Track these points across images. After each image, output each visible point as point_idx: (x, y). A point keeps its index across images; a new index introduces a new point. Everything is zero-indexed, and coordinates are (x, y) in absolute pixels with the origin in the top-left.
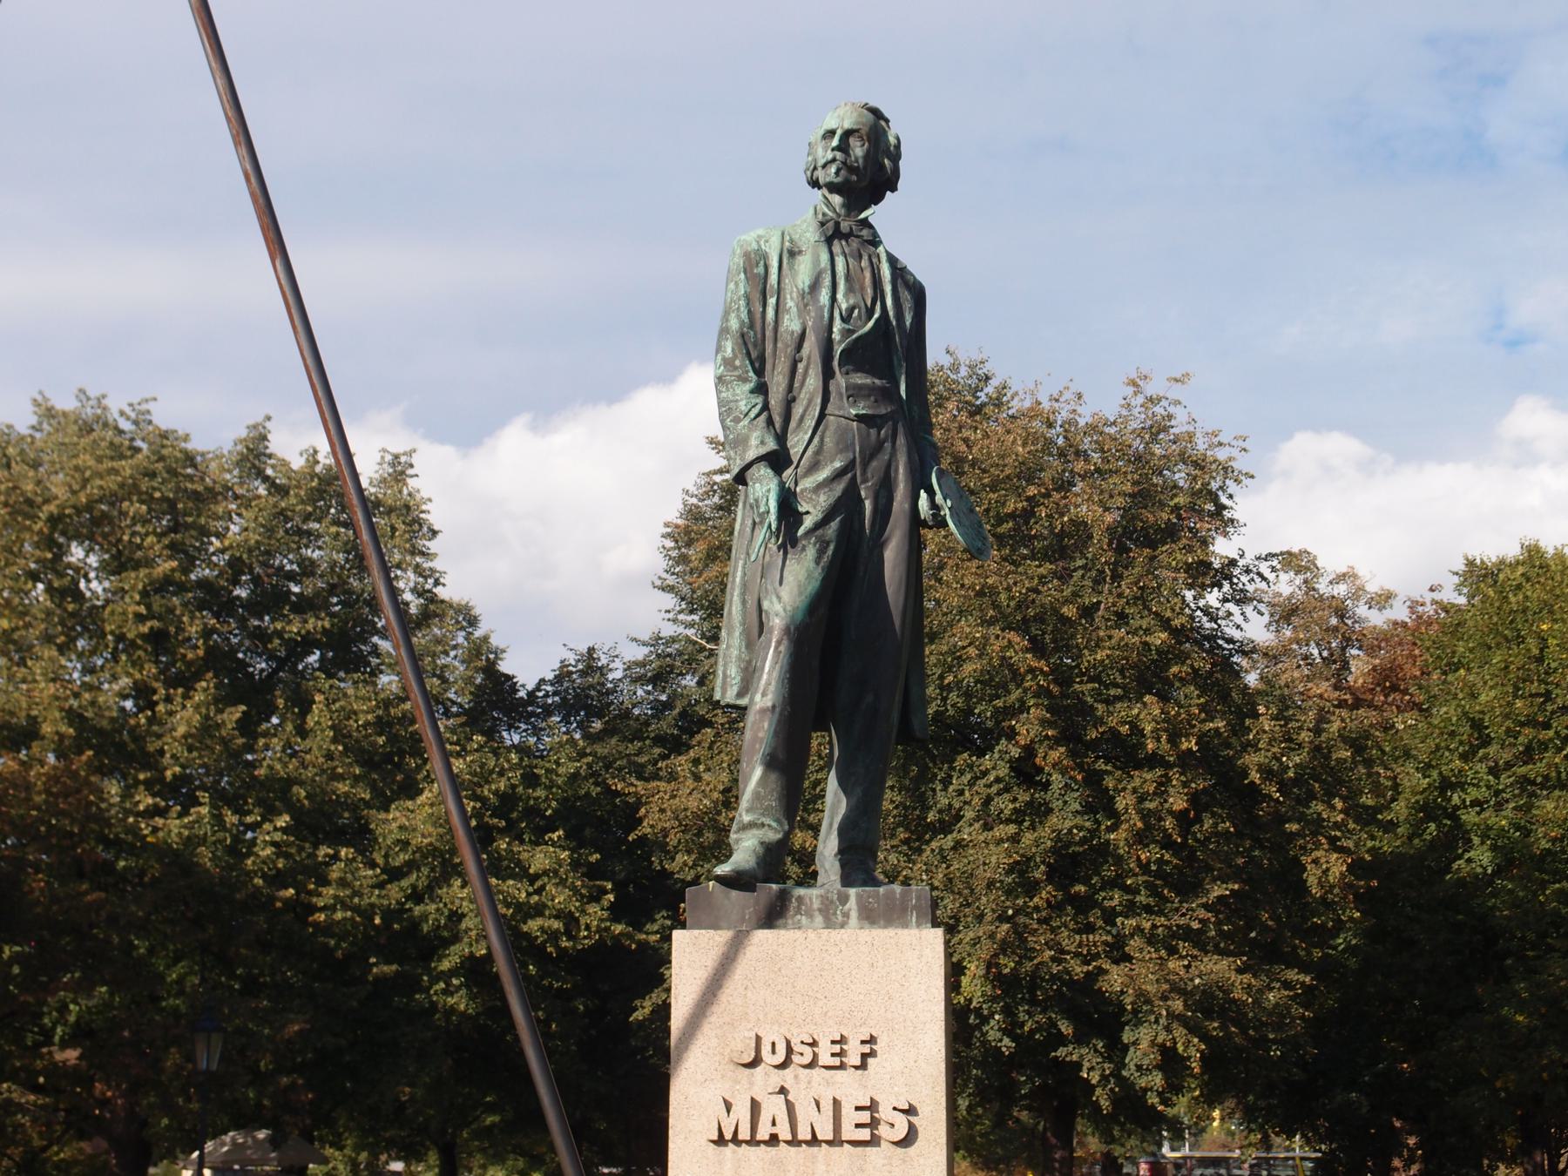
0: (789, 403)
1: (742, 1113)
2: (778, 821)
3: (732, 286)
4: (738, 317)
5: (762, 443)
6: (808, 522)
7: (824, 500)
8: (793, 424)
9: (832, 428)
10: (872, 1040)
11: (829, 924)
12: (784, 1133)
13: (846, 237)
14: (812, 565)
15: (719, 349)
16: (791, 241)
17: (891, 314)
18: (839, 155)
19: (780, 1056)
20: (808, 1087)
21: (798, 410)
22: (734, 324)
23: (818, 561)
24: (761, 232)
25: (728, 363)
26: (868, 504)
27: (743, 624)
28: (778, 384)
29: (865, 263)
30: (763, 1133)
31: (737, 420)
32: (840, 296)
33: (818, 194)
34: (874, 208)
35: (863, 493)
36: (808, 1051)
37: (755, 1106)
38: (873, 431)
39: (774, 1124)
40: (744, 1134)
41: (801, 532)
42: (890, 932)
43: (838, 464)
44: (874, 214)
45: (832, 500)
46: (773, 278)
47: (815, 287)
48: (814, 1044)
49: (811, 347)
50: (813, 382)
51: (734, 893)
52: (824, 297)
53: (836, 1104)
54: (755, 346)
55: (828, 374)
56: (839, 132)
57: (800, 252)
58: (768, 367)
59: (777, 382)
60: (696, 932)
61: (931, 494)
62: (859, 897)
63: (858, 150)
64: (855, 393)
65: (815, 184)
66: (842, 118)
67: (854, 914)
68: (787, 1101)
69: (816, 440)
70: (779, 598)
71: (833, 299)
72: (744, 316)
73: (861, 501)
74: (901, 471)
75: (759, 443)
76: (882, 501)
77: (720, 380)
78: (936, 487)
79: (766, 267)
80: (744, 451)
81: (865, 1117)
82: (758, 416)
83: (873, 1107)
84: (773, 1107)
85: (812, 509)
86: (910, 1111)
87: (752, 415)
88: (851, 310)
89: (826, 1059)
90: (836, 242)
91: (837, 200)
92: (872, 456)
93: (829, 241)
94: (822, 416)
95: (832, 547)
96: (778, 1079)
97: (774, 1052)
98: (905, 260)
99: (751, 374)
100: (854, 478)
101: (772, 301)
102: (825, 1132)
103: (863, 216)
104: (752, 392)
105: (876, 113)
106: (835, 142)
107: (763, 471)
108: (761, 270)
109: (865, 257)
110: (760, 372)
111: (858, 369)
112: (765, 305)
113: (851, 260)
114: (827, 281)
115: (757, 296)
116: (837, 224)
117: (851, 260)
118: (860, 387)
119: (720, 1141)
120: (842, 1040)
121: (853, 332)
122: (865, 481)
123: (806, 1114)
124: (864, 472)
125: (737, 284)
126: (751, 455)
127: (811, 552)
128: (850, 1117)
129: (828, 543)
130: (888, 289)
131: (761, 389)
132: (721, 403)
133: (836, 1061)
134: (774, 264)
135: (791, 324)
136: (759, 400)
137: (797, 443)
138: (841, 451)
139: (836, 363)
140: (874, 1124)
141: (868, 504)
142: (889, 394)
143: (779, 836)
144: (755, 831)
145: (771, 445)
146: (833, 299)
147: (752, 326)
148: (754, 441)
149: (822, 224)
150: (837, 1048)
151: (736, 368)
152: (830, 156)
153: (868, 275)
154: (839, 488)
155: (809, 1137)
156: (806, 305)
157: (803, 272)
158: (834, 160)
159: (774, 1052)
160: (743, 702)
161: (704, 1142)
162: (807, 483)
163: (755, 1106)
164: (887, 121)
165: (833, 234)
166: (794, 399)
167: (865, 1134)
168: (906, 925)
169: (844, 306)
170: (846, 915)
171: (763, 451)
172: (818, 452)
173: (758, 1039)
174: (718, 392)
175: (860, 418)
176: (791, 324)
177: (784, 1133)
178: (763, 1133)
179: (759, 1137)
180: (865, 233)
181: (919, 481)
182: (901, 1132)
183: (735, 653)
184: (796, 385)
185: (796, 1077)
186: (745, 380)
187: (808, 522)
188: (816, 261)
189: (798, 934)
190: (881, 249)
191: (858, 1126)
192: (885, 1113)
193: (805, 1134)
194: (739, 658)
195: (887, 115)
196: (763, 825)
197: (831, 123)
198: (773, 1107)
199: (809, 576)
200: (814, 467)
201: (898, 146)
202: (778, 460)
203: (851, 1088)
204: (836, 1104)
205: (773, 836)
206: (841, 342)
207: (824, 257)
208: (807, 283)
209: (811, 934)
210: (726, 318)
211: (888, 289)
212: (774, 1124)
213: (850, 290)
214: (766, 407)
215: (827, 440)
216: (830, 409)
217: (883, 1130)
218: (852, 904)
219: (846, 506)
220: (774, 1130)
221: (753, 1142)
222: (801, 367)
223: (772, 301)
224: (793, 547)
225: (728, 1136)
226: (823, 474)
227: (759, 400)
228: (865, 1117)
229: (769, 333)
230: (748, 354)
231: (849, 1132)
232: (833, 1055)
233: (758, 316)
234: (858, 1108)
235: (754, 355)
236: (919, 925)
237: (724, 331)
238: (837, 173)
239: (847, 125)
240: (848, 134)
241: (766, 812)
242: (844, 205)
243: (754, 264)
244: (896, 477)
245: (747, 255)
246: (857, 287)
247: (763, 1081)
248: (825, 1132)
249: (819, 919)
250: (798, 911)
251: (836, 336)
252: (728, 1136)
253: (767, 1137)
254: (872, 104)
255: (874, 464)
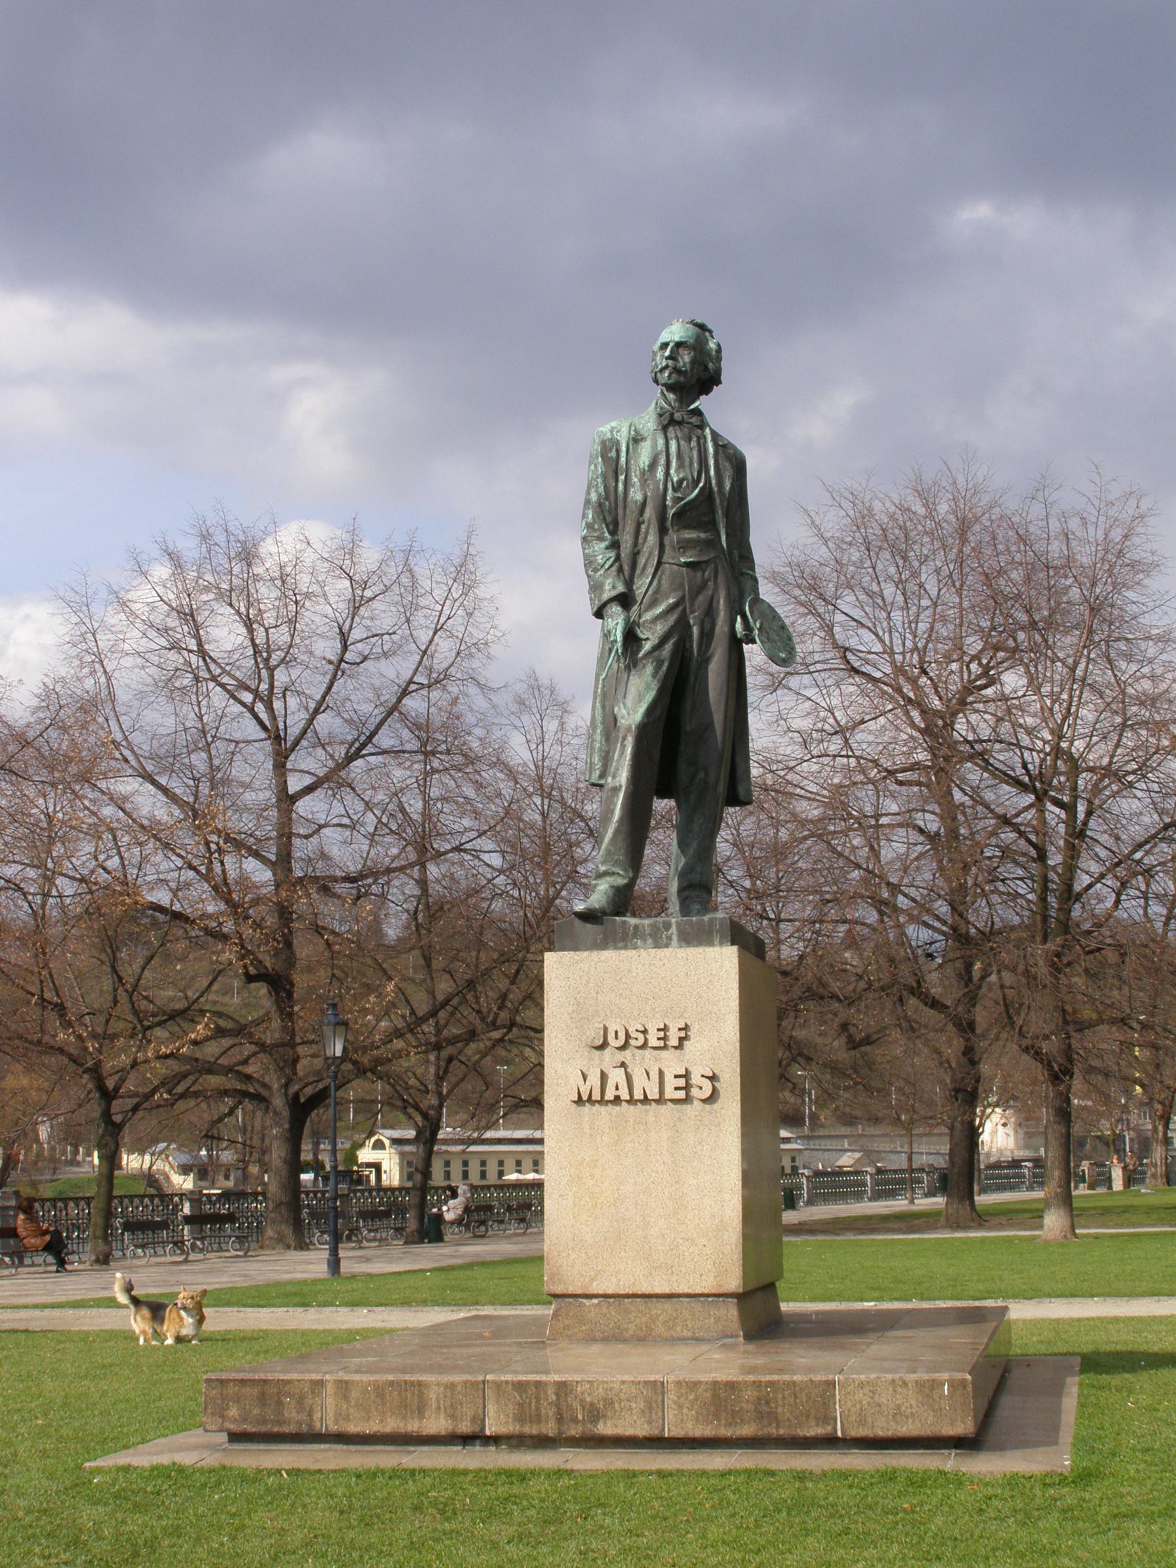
0: (635, 555)
1: (594, 1080)
2: (625, 870)
3: (592, 467)
4: (597, 491)
5: (614, 587)
6: (647, 646)
7: (660, 628)
8: (638, 571)
9: (667, 573)
10: (686, 1028)
11: (657, 945)
12: (625, 1095)
13: (680, 423)
14: (650, 678)
15: (584, 516)
16: (635, 431)
17: (714, 482)
18: (670, 362)
19: (621, 1042)
20: (640, 1063)
21: (642, 561)
22: (594, 497)
23: (654, 676)
24: (613, 424)
25: (589, 526)
26: (695, 631)
27: (603, 723)
28: (626, 542)
29: (693, 444)
30: (610, 1095)
31: (596, 570)
32: (672, 471)
33: (659, 389)
34: (703, 398)
35: (691, 621)
36: (641, 1036)
37: (604, 1077)
38: (699, 574)
39: (617, 1088)
40: (596, 1096)
41: (641, 655)
42: (700, 950)
43: (671, 601)
44: (702, 403)
45: (666, 628)
46: (623, 459)
47: (653, 465)
48: (645, 1032)
49: (649, 513)
50: (652, 539)
51: (589, 926)
52: (660, 473)
53: (661, 1073)
54: (610, 512)
55: (663, 531)
56: (671, 345)
57: (643, 439)
58: (620, 527)
59: (626, 539)
60: (561, 953)
61: (744, 617)
62: (678, 924)
63: (686, 358)
64: (684, 546)
65: (656, 381)
66: (675, 332)
67: (675, 937)
68: (627, 1074)
69: (655, 583)
70: (624, 704)
71: (667, 474)
72: (601, 490)
73: (689, 627)
74: (722, 602)
75: (612, 587)
76: (708, 626)
77: (584, 539)
78: (748, 613)
79: (618, 452)
80: (601, 594)
81: (682, 1082)
82: (611, 566)
83: (687, 1075)
84: (617, 1076)
85: (650, 637)
86: (713, 1078)
87: (607, 566)
88: (681, 481)
89: (653, 1042)
90: (671, 429)
91: (671, 396)
92: (699, 592)
93: (665, 429)
94: (659, 563)
95: (666, 664)
96: (620, 1056)
97: (616, 1038)
98: (729, 436)
99: (607, 534)
100: (684, 610)
101: (622, 478)
102: (653, 1094)
103: (692, 407)
104: (607, 548)
105: (702, 327)
106: (667, 353)
107: (616, 609)
108: (613, 454)
109: (695, 439)
110: (613, 533)
111: (688, 527)
112: (617, 481)
113: (682, 442)
114: (662, 461)
115: (611, 474)
116: (672, 415)
117: (682, 442)
118: (689, 541)
119: (579, 1101)
120: (665, 1029)
121: (683, 499)
122: (692, 612)
123: (640, 1082)
124: (692, 605)
125: (596, 466)
126: (606, 596)
127: (649, 669)
128: (671, 1083)
129: (663, 662)
130: (711, 462)
131: (615, 545)
132: (586, 556)
133: (661, 1043)
134: (624, 449)
135: (636, 495)
136: (612, 554)
137: (641, 585)
138: (675, 590)
139: (669, 523)
140: (687, 1087)
141: (695, 631)
142: (713, 543)
143: (626, 881)
144: (608, 879)
145: (621, 588)
146: (667, 474)
147: (607, 498)
148: (607, 587)
149: (661, 416)
150: (662, 1034)
151: (595, 530)
152: (664, 364)
153: (695, 453)
154: (672, 619)
155: (642, 1097)
156: (646, 481)
157: (644, 457)
158: (667, 367)
159: (616, 1038)
160: (602, 782)
161: (569, 1103)
162: (648, 616)
163: (604, 1077)
164: (710, 332)
165: (668, 422)
166: (638, 553)
167: (681, 1094)
168: (711, 944)
169: (675, 479)
170: (669, 938)
171: (614, 593)
172: (657, 592)
173: (605, 1029)
174: (584, 549)
175: (688, 565)
176: (636, 495)
177: (625, 1095)
178: (610, 1095)
179: (606, 1098)
180: (694, 420)
181: (736, 608)
182: (707, 1092)
183: (597, 745)
184: (640, 541)
185: (633, 1055)
186: (601, 539)
187: (647, 646)
188: (655, 445)
189: (634, 952)
190: (708, 430)
191: (676, 1089)
192: (696, 1079)
193: (638, 1095)
194: (600, 749)
195: (710, 327)
196: (614, 873)
197: (665, 337)
198: (617, 1076)
199: (648, 688)
200: (654, 603)
201: (719, 350)
202: (625, 600)
203: (672, 1064)
204: (661, 1073)
205: (621, 882)
206: (672, 507)
207: (661, 442)
208: (647, 463)
209: (643, 952)
210: (588, 493)
211: (711, 462)
212: (617, 1088)
213: (681, 466)
214: (618, 558)
215: (663, 582)
216: (665, 559)
217: (695, 1092)
218: (674, 930)
219: (682, 627)
220: (617, 1093)
221: (602, 1101)
222: (643, 527)
223: (622, 478)
224: (635, 667)
225: (585, 1098)
226: (659, 610)
227: (612, 554)
228: (682, 1082)
229: (620, 503)
230: (604, 519)
231: (670, 1093)
232: (659, 1039)
233: (612, 489)
234: (676, 1076)
235: (609, 519)
236: (721, 944)
237: (588, 502)
238: (669, 377)
239: (677, 339)
240: (679, 345)
241: (616, 863)
242: (676, 400)
243: (609, 452)
244: (718, 607)
245: (603, 443)
246: (687, 463)
247: (609, 1057)
248: (653, 1094)
249: (650, 941)
250: (635, 935)
251: (669, 503)
252: (585, 1098)
253: (612, 1098)
254: (699, 321)
255: (701, 598)
